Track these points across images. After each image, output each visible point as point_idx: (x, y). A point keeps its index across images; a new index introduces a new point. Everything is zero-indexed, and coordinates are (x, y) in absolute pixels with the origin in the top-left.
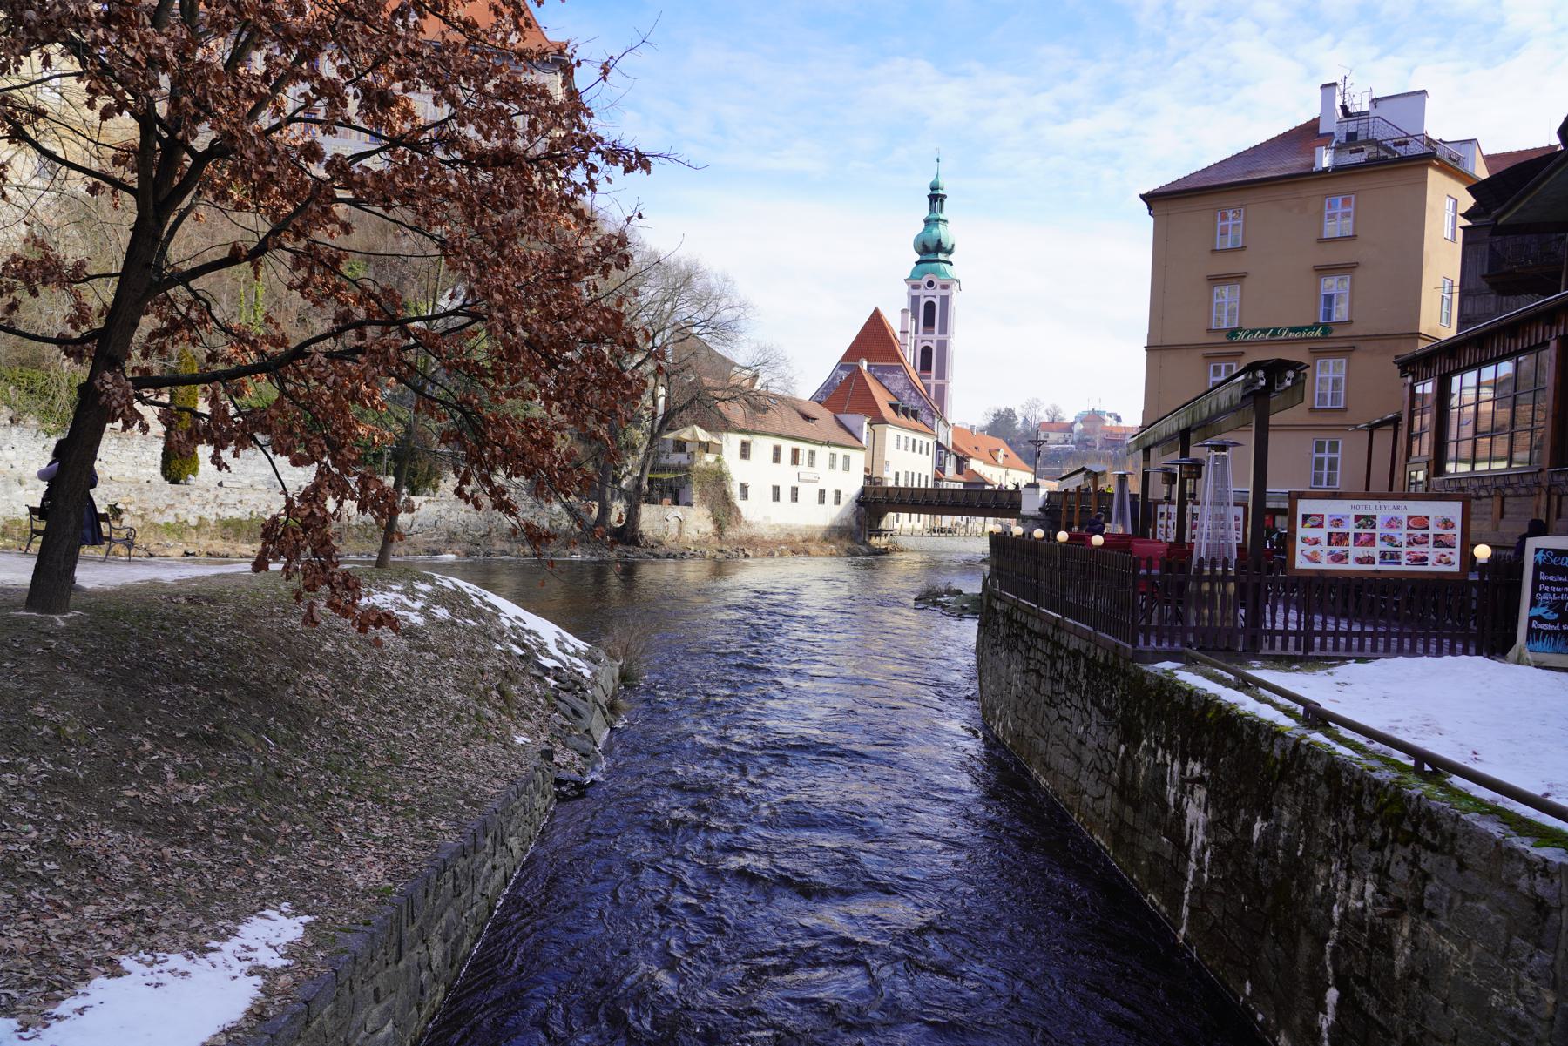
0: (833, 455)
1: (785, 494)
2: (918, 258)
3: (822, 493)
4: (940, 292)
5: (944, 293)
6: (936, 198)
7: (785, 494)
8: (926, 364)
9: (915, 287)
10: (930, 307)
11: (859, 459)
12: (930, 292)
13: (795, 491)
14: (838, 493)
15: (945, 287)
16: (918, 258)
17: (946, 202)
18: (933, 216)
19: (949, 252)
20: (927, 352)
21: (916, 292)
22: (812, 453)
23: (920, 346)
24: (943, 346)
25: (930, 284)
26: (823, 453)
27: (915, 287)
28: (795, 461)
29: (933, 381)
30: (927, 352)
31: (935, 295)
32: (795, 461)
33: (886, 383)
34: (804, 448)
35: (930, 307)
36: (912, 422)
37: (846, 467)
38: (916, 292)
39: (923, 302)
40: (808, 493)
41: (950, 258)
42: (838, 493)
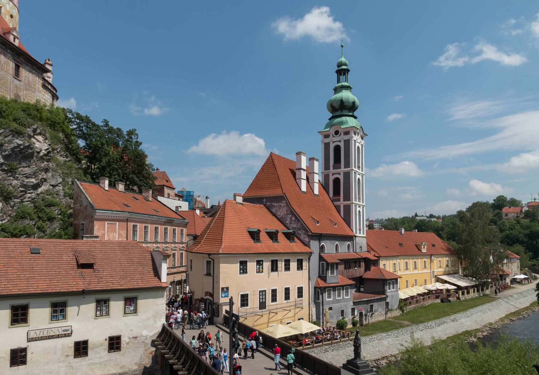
2: (331, 115)
5: (346, 137)
9: (327, 136)
10: (337, 149)
12: (337, 138)
15: (347, 133)
21: (327, 140)
23: (331, 178)
24: (347, 176)
25: (337, 133)
27: (327, 136)
29: (342, 203)
31: (340, 141)
33: (274, 210)
35: (337, 149)
38: (327, 140)
39: (332, 146)
41: (355, 114)
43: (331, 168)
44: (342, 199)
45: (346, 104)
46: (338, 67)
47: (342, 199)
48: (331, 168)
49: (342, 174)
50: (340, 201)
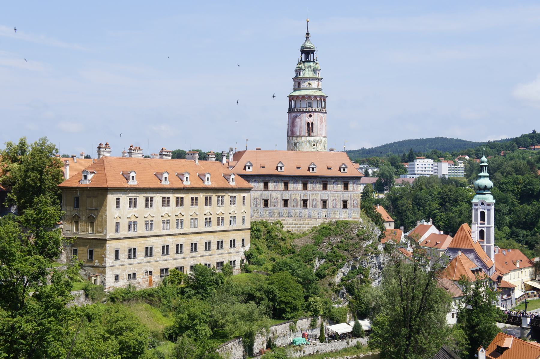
12: (483, 207)
39: (479, 211)
44: (485, 243)
47: (485, 243)
50: (483, 242)
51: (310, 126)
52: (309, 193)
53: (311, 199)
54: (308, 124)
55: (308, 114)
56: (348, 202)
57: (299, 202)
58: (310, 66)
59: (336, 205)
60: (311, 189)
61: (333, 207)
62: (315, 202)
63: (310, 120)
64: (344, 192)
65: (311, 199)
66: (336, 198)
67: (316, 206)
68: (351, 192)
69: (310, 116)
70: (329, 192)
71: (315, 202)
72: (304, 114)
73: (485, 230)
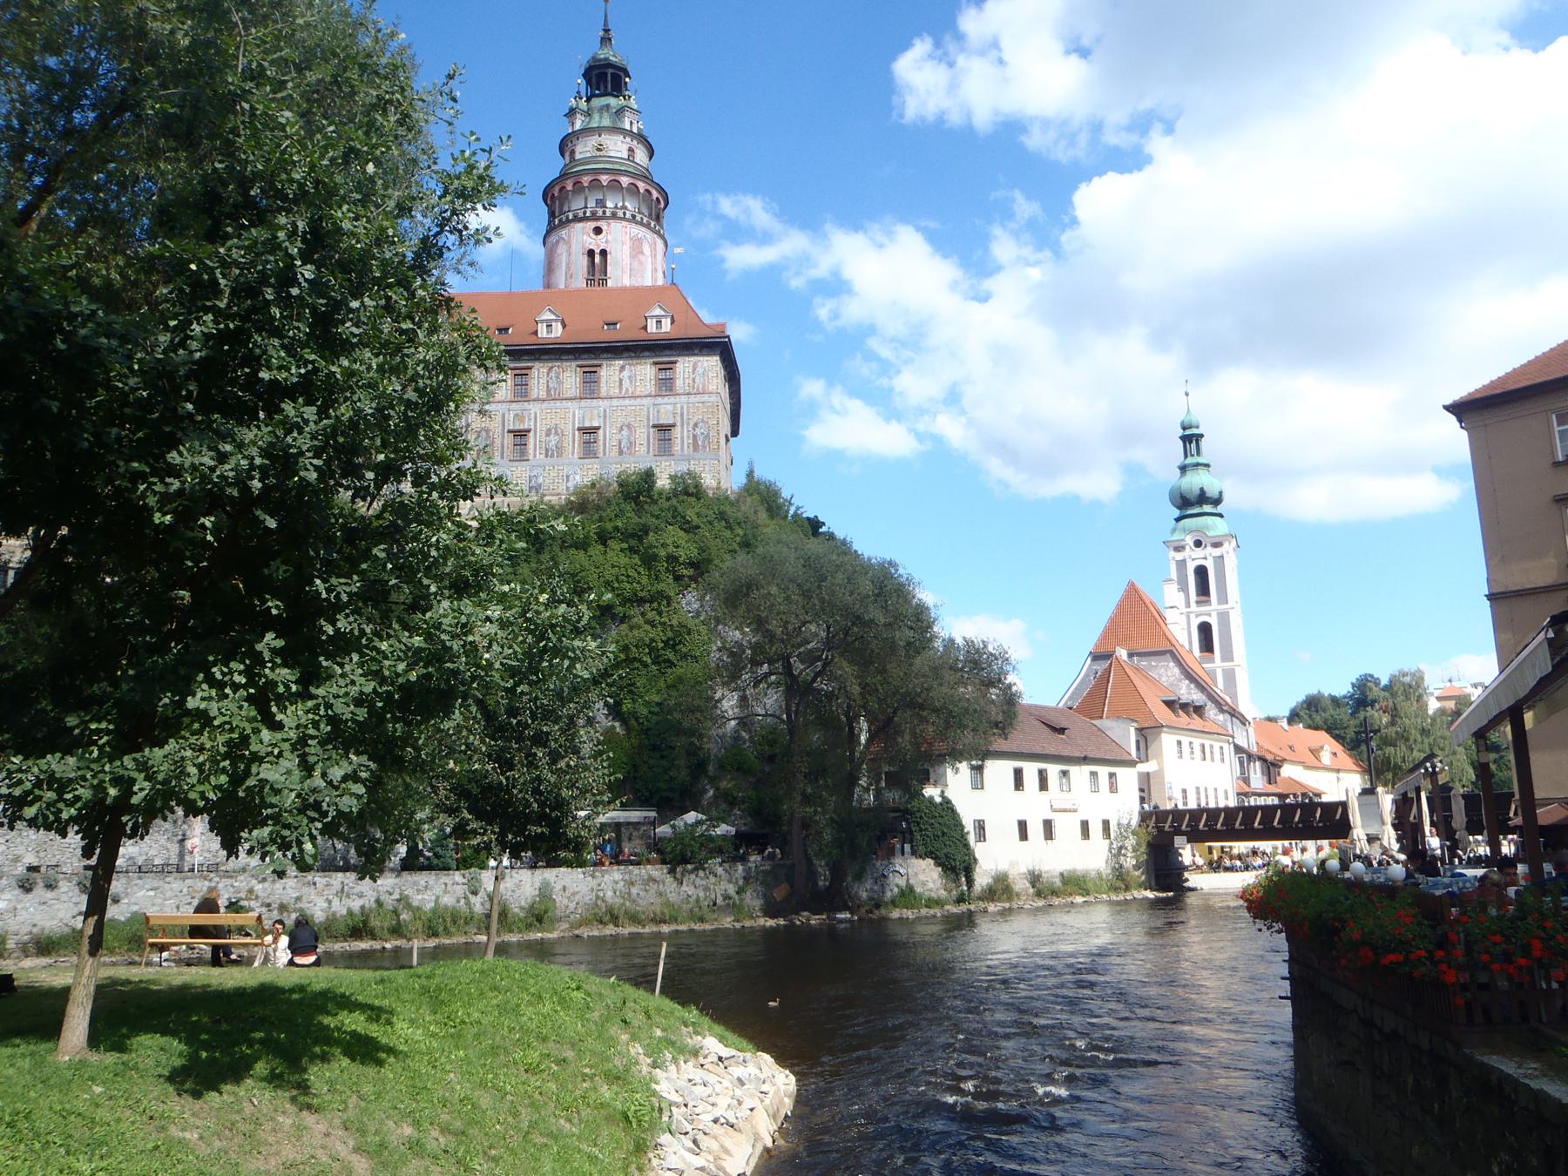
0: (1094, 774)
1: (1035, 830)
2: (1177, 513)
3: (1085, 825)
4: (1210, 551)
6: (1191, 439)
7: (1035, 830)
8: (1207, 645)
10: (1201, 572)
11: (1128, 778)
12: (1199, 552)
13: (1048, 826)
14: (1106, 824)
16: (1177, 513)
17: (1204, 443)
18: (1190, 460)
19: (1217, 502)
20: (1205, 629)
21: (1179, 556)
22: (1065, 773)
23: (1195, 623)
24: (1224, 618)
25: (1198, 544)
26: (1080, 773)
28: (1043, 785)
29: (1217, 663)
30: (1205, 629)
32: (1043, 785)
34: (1053, 770)
35: (1201, 572)
36: (1196, 722)
37: (1113, 788)
38: (1179, 556)
39: (1191, 567)
40: (1067, 827)
41: (1219, 509)
42: (1106, 824)
43: (1193, 604)
45: (1209, 494)
46: (1184, 429)
48: (1193, 604)
49: (1214, 614)
51: (597, 259)
52: (534, 408)
53: (541, 428)
54: (591, 253)
55: (592, 225)
56: (677, 432)
57: (498, 442)
58: (608, 106)
59: (631, 444)
60: (543, 395)
61: (621, 453)
62: (553, 440)
63: (596, 243)
64: (660, 400)
65: (541, 428)
66: (629, 419)
67: (559, 450)
68: (684, 399)
69: (598, 231)
70: (606, 403)
71: (553, 440)
72: (580, 225)
73: (1214, 621)
